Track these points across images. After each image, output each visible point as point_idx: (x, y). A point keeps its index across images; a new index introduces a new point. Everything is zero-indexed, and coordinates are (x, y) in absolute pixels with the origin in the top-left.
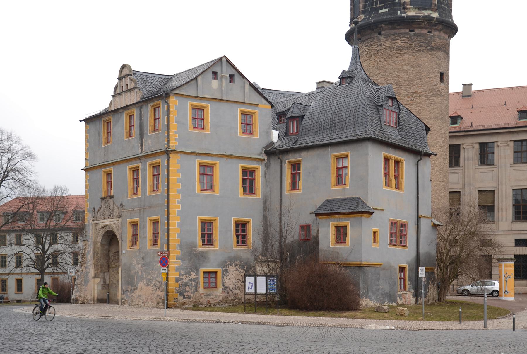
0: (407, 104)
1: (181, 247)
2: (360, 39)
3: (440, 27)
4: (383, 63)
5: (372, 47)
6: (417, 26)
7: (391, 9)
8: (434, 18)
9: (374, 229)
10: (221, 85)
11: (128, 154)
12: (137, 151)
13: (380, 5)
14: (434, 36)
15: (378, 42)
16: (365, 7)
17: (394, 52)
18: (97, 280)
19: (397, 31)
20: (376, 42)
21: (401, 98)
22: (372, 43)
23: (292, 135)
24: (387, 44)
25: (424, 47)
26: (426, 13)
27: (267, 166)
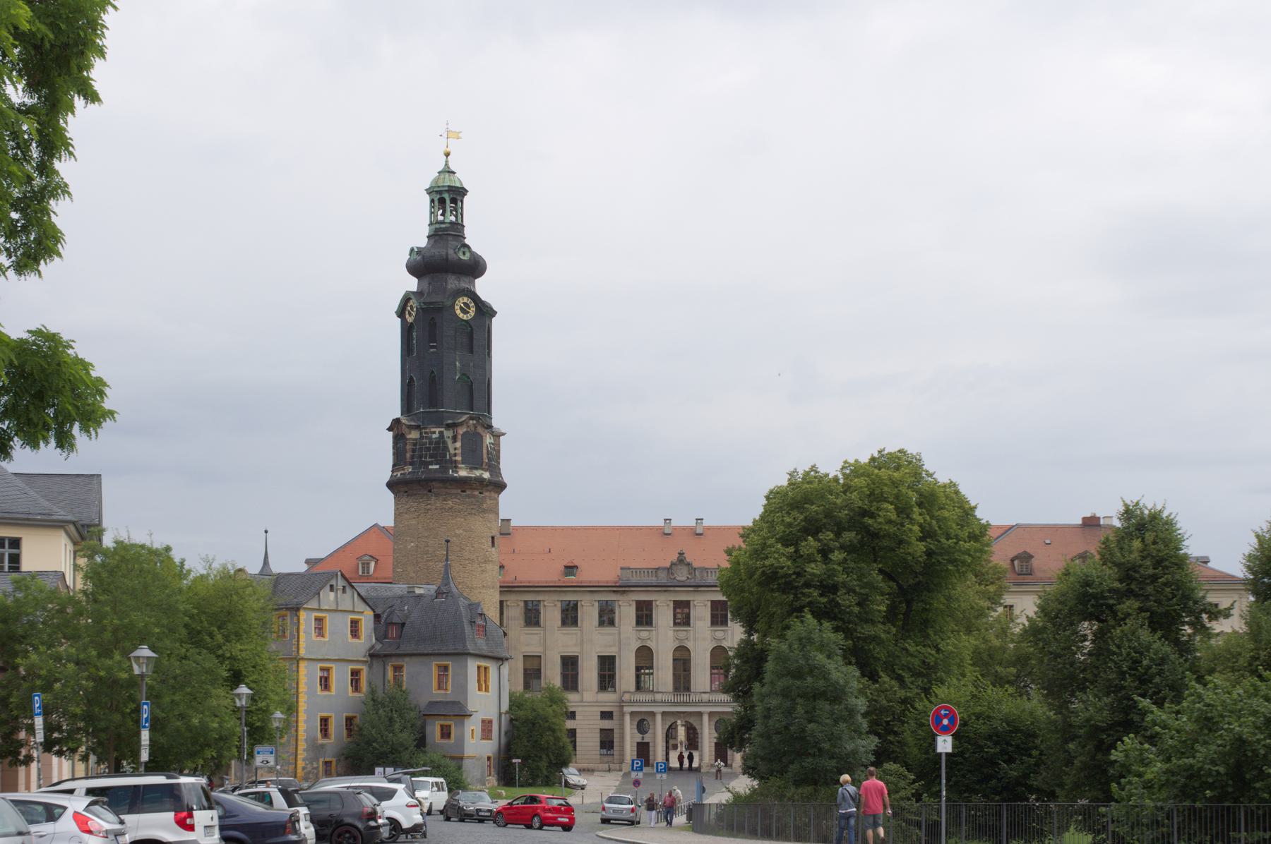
1: (306, 740)
2: (406, 492)
9: (472, 728)
14: (485, 497)
16: (412, 457)
23: (394, 639)
24: (438, 504)
26: (477, 473)
27: (370, 667)
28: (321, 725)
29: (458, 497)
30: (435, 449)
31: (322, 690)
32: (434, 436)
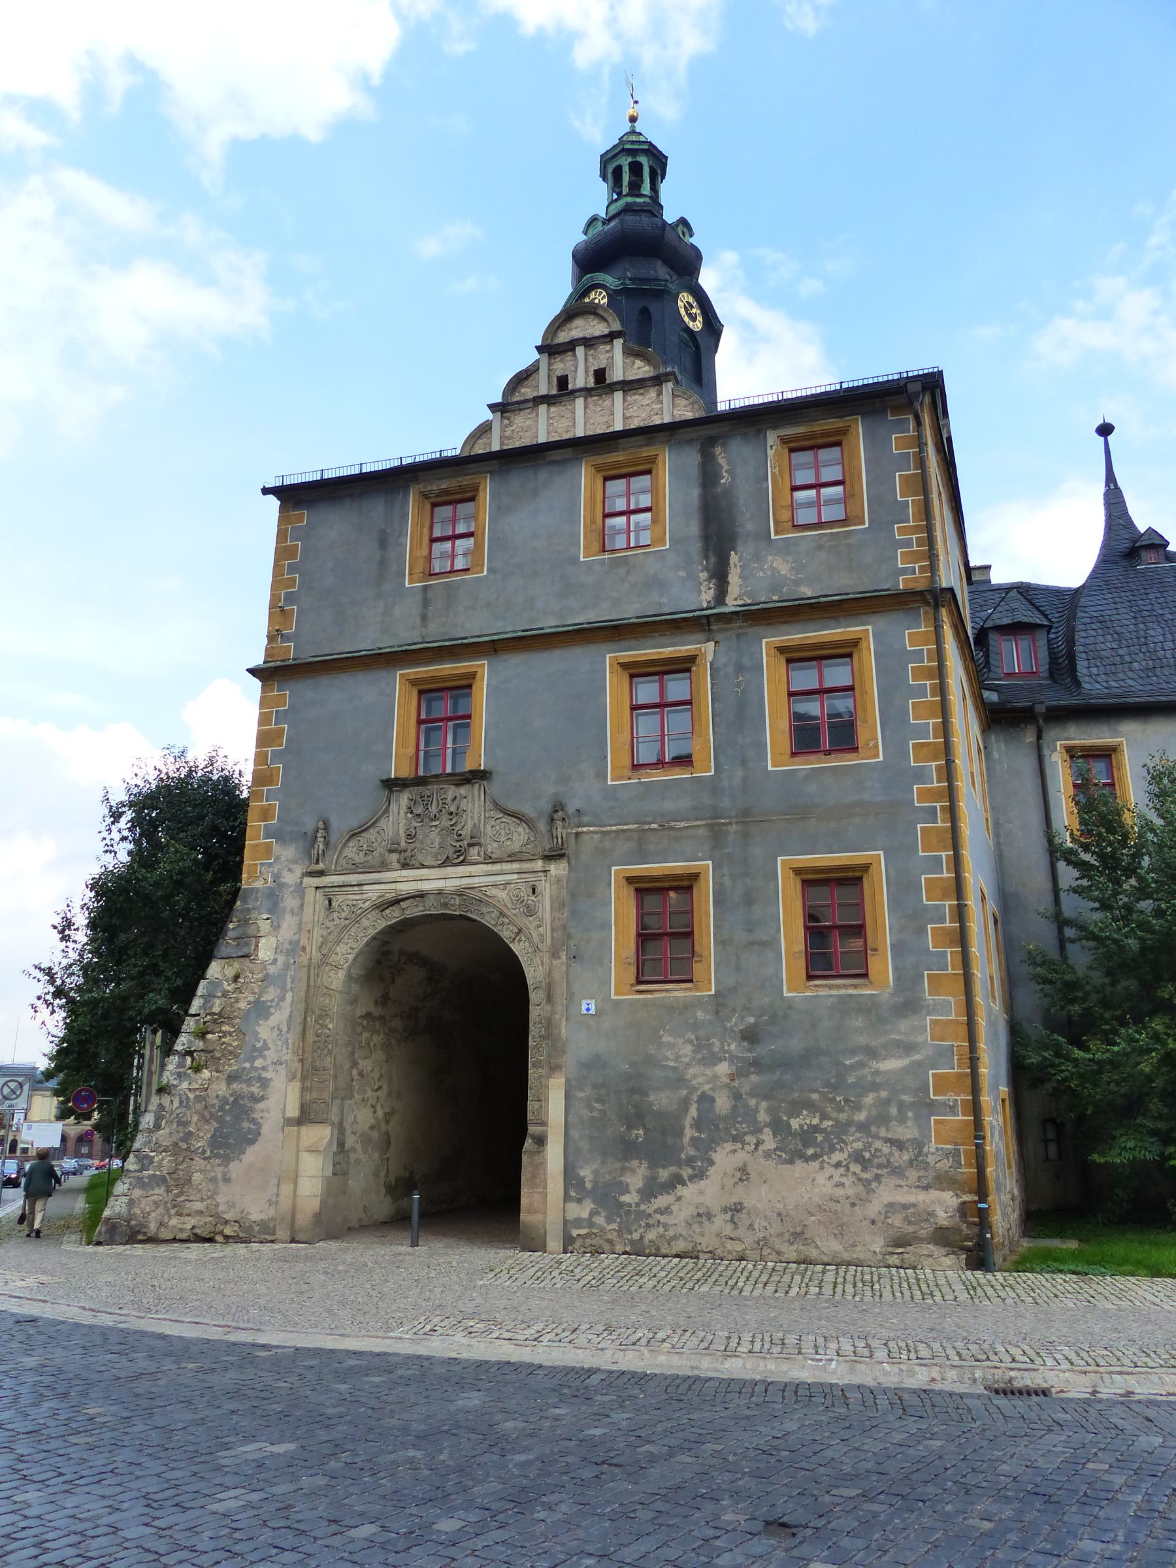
18: (320, 1135)
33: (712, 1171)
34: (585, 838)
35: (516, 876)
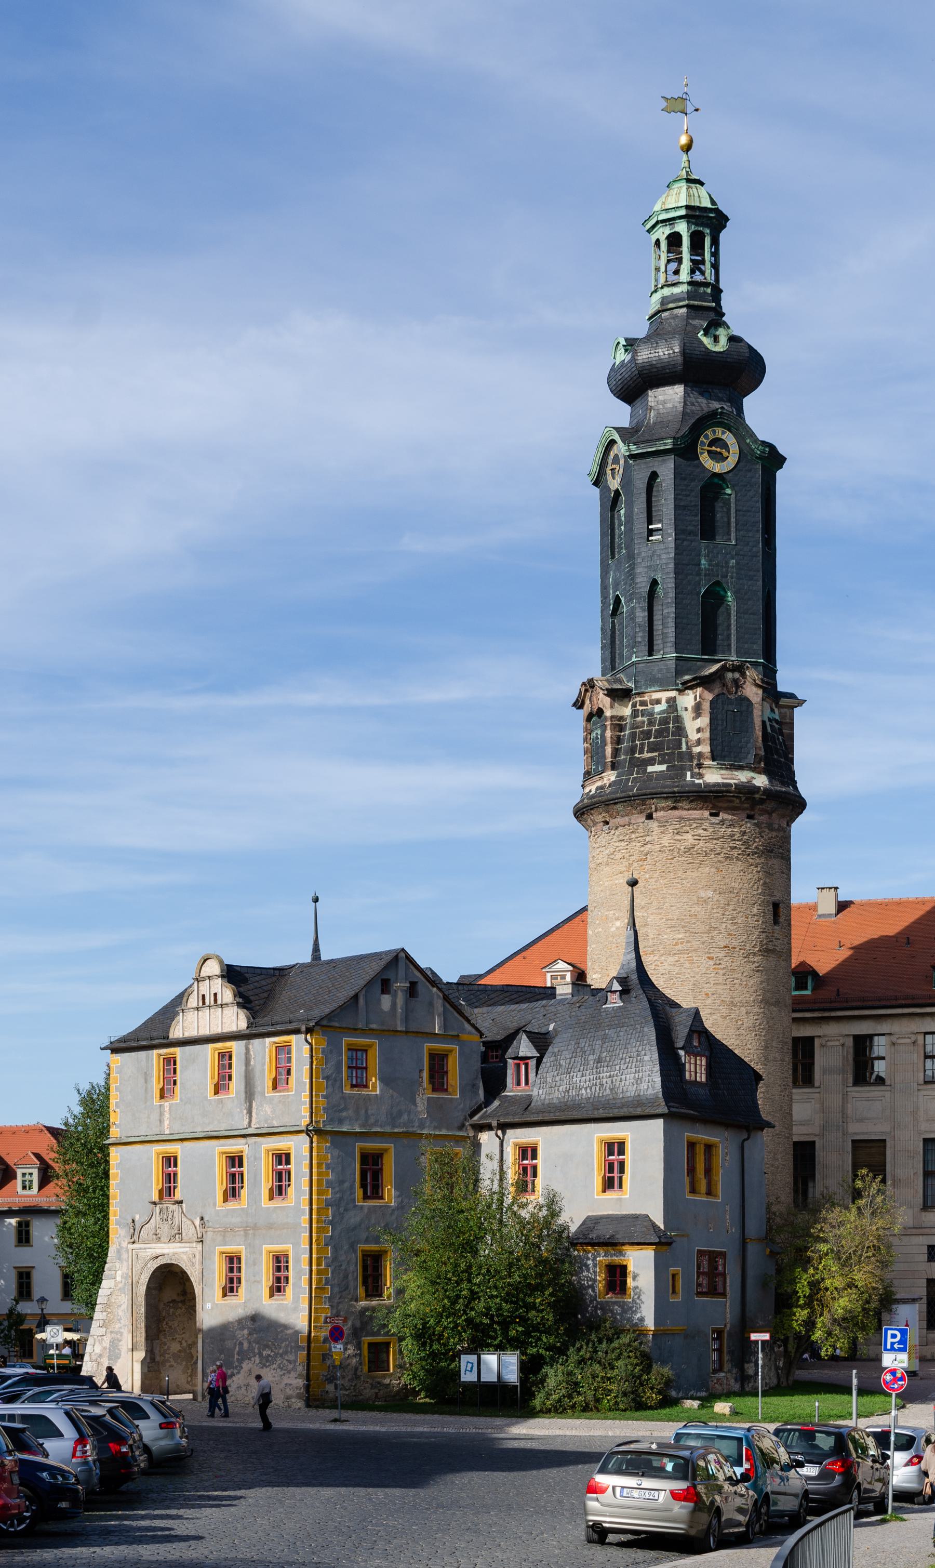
0: (708, 972)
3: (769, 805)
4: (656, 882)
5: (634, 844)
6: (726, 805)
7: (672, 766)
8: (759, 788)
10: (394, 1004)
11: (221, 1126)
12: (240, 1122)
13: (650, 755)
15: (646, 836)
16: (616, 752)
17: (680, 859)
19: (684, 813)
20: (642, 834)
21: (695, 959)
22: (633, 836)
24: (666, 840)
25: (740, 849)
26: (743, 776)
28: (365, 1268)
29: (706, 825)
30: (659, 733)
31: (366, 1197)
32: (658, 708)
33: (242, 1371)
34: (208, 1233)
35: (188, 1249)
